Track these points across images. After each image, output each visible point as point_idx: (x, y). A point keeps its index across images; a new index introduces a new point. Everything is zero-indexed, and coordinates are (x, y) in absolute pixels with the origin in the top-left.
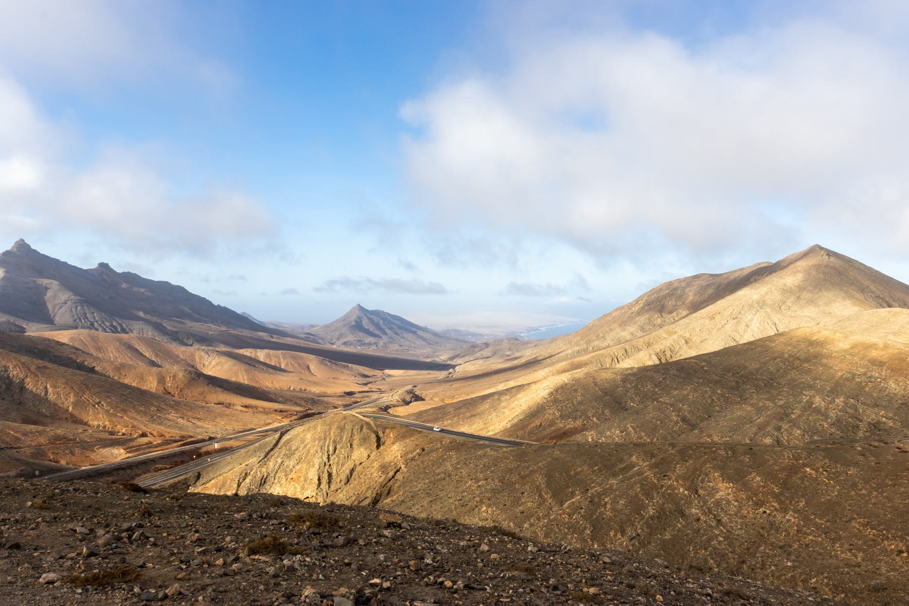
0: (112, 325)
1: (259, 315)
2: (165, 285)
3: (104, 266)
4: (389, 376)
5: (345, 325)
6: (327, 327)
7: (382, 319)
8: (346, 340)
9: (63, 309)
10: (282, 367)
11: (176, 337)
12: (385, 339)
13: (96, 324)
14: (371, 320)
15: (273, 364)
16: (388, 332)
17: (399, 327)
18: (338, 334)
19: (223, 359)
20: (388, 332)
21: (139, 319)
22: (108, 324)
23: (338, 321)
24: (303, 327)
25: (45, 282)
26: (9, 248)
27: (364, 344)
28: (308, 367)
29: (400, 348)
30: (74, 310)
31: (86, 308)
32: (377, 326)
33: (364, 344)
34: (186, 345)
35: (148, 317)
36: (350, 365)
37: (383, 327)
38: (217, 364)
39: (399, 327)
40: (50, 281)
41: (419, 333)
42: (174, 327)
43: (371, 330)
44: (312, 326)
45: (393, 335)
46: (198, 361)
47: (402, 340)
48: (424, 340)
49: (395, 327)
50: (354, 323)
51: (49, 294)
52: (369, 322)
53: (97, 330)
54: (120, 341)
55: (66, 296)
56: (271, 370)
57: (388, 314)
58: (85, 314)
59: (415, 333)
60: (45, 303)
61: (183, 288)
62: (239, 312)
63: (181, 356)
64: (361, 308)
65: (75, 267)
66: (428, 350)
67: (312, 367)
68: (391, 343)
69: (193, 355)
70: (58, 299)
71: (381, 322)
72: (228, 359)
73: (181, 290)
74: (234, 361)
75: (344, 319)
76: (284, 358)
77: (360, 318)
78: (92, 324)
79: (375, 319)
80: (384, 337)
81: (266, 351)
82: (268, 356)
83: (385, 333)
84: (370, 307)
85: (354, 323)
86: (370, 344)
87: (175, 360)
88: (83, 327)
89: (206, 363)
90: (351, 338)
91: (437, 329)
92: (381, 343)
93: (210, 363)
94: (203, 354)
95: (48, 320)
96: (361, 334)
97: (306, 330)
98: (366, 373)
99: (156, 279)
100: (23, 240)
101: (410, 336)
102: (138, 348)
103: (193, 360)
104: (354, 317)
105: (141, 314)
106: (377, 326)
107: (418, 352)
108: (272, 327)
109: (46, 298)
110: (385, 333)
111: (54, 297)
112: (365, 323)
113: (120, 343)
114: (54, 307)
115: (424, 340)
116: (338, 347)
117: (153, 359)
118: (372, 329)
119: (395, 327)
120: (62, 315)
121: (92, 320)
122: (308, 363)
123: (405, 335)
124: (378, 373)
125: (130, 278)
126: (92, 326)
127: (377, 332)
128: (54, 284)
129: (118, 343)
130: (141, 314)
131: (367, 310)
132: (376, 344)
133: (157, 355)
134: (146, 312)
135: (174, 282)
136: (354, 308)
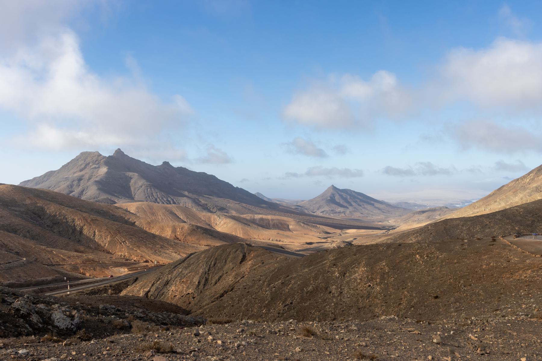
0: (168, 200)
1: (269, 195)
3: (166, 164)
4: (346, 233)
5: (323, 200)
6: (311, 201)
7: (350, 195)
8: (323, 210)
9: (140, 191)
11: (205, 208)
12: (351, 208)
14: (341, 196)
16: (353, 204)
17: (361, 200)
18: (318, 206)
19: (228, 220)
20: (353, 204)
21: (184, 196)
22: (165, 199)
24: (297, 202)
25: (130, 174)
26: (112, 154)
27: (336, 213)
29: (361, 215)
30: (146, 191)
31: (153, 190)
32: (346, 200)
33: (336, 213)
34: (211, 212)
35: (190, 195)
36: (318, 226)
37: (350, 201)
38: (225, 223)
39: (361, 200)
40: (133, 173)
41: (377, 205)
42: (206, 201)
43: (341, 203)
44: (303, 201)
45: (357, 206)
46: (213, 221)
48: (379, 209)
49: (358, 200)
51: (132, 181)
52: (341, 197)
53: (159, 203)
54: (166, 208)
55: (142, 182)
56: (260, 228)
57: (354, 192)
58: (152, 194)
59: (373, 205)
60: (130, 187)
61: (214, 176)
62: (253, 192)
63: (203, 218)
64: (334, 188)
65: (149, 165)
66: (382, 217)
68: (355, 211)
70: (137, 183)
71: (348, 197)
72: (231, 220)
74: (235, 222)
77: (333, 195)
78: (156, 200)
79: (344, 195)
80: (350, 208)
83: (351, 205)
86: (340, 212)
89: (218, 223)
90: (327, 208)
91: (392, 202)
92: (348, 212)
93: (220, 223)
94: (216, 217)
95: (130, 197)
96: (334, 206)
99: (198, 171)
100: (119, 149)
101: (369, 207)
102: (176, 213)
103: (210, 221)
104: (329, 194)
105: (186, 193)
106: (346, 200)
107: (375, 218)
109: (131, 184)
110: (351, 205)
111: (135, 183)
112: (337, 198)
113: (166, 210)
114: (135, 189)
115: (379, 209)
118: (342, 202)
119: (358, 200)
120: (139, 194)
121: (156, 197)
123: (366, 206)
127: (345, 204)
128: (135, 176)
129: (164, 210)
130: (186, 193)
131: (339, 189)
132: (344, 212)
134: (189, 192)
135: (209, 173)
136: (329, 188)
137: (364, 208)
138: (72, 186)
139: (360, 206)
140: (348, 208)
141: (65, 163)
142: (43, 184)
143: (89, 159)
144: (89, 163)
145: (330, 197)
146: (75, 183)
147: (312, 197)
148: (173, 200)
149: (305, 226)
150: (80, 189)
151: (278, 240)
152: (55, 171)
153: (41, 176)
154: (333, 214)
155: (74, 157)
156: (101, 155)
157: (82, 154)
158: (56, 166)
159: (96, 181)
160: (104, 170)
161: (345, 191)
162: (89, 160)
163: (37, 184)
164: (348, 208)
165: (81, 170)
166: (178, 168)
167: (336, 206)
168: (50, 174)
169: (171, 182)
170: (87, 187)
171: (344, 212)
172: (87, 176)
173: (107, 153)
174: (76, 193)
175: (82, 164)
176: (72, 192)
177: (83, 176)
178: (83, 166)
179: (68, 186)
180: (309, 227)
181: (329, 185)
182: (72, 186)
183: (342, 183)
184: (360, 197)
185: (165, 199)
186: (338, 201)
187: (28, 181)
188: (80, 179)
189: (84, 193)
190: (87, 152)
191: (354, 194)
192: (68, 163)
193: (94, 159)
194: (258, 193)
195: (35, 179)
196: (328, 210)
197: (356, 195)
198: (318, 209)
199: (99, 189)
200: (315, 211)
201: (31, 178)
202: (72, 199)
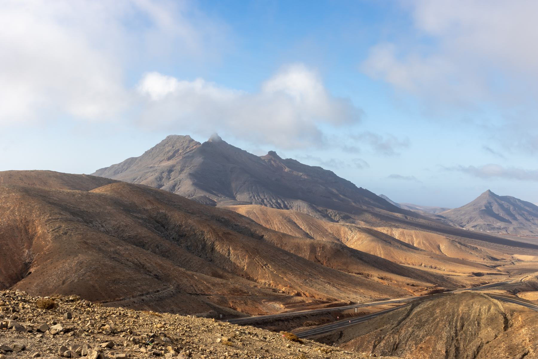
0: (277, 202)
1: (395, 198)
2: (318, 171)
4: (519, 260)
5: (475, 210)
6: (457, 210)
7: (513, 205)
8: (475, 224)
10: (415, 245)
12: (515, 224)
13: (265, 200)
14: (501, 206)
15: (407, 242)
16: (519, 217)
19: (363, 236)
20: (519, 217)
22: (274, 201)
23: (469, 205)
24: (435, 210)
26: (207, 140)
27: (494, 228)
28: (439, 247)
29: (531, 234)
32: (507, 211)
33: (494, 228)
34: (333, 221)
37: (514, 213)
38: (359, 239)
39: (530, 213)
43: (501, 215)
44: (443, 209)
45: (524, 221)
47: (533, 226)
50: (484, 208)
53: (266, 205)
54: (283, 215)
57: (519, 200)
61: (332, 173)
62: (378, 194)
63: (329, 231)
64: (491, 194)
65: (252, 154)
67: (442, 247)
68: (521, 228)
69: (338, 231)
72: (368, 235)
73: (331, 174)
75: (474, 203)
76: (417, 237)
77: (490, 203)
78: (263, 201)
79: (506, 204)
80: (514, 222)
81: (401, 230)
82: (402, 234)
83: (515, 219)
84: (500, 194)
85: (484, 208)
86: (499, 229)
87: (324, 233)
88: (256, 203)
89: (350, 238)
90: (480, 222)
92: (511, 228)
93: (353, 238)
94: (347, 229)
96: (491, 219)
97: (438, 213)
98: (495, 256)
102: (296, 222)
103: (339, 234)
104: (484, 202)
106: (507, 211)
108: (406, 208)
110: (515, 219)
112: (495, 208)
113: (283, 217)
116: (469, 228)
117: (308, 232)
118: (502, 214)
122: (438, 243)
124: (508, 257)
125: (291, 163)
126: (262, 203)
127: (507, 217)
129: (281, 217)
131: (497, 196)
132: (506, 229)
133: (310, 229)
136: (484, 194)
137: (534, 224)
138: (161, 178)
139: (529, 220)
140: (511, 223)
141: (149, 148)
142: (124, 173)
143: (178, 145)
144: (178, 150)
145: (486, 207)
146: (165, 175)
147: (458, 206)
148: (284, 203)
149: (463, 247)
150: (171, 183)
151: (433, 266)
152: (136, 158)
153: (120, 164)
154: (489, 230)
155: (159, 141)
156: (193, 140)
157: (169, 138)
158: (138, 153)
159: (190, 174)
160: (198, 160)
161: (507, 199)
162: (178, 146)
163: (116, 173)
164: (511, 223)
165: (169, 159)
166: (287, 159)
167: (495, 219)
168: (131, 162)
169: (280, 179)
170: (180, 181)
171: (506, 229)
172: (178, 168)
173: (202, 140)
174: (166, 187)
175: (168, 152)
176: (162, 186)
177: (174, 166)
178: (171, 154)
179: (156, 179)
180: (467, 250)
181: (486, 190)
182: (161, 178)
183: (504, 188)
184: (528, 209)
185: (274, 201)
186: (497, 213)
187: (106, 168)
188: (170, 171)
189: (176, 188)
190: (175, 136)
191: (519, 203)
192: (153, 149)
193: (185, 145)
194: (382, 195)
195: (113, 166)
196: (482, 223)
197: (522, 206)
198: (468, 223)
199: (194, 184)
200: (464, 224)
201: (109, 166)
202: (162, 193)
